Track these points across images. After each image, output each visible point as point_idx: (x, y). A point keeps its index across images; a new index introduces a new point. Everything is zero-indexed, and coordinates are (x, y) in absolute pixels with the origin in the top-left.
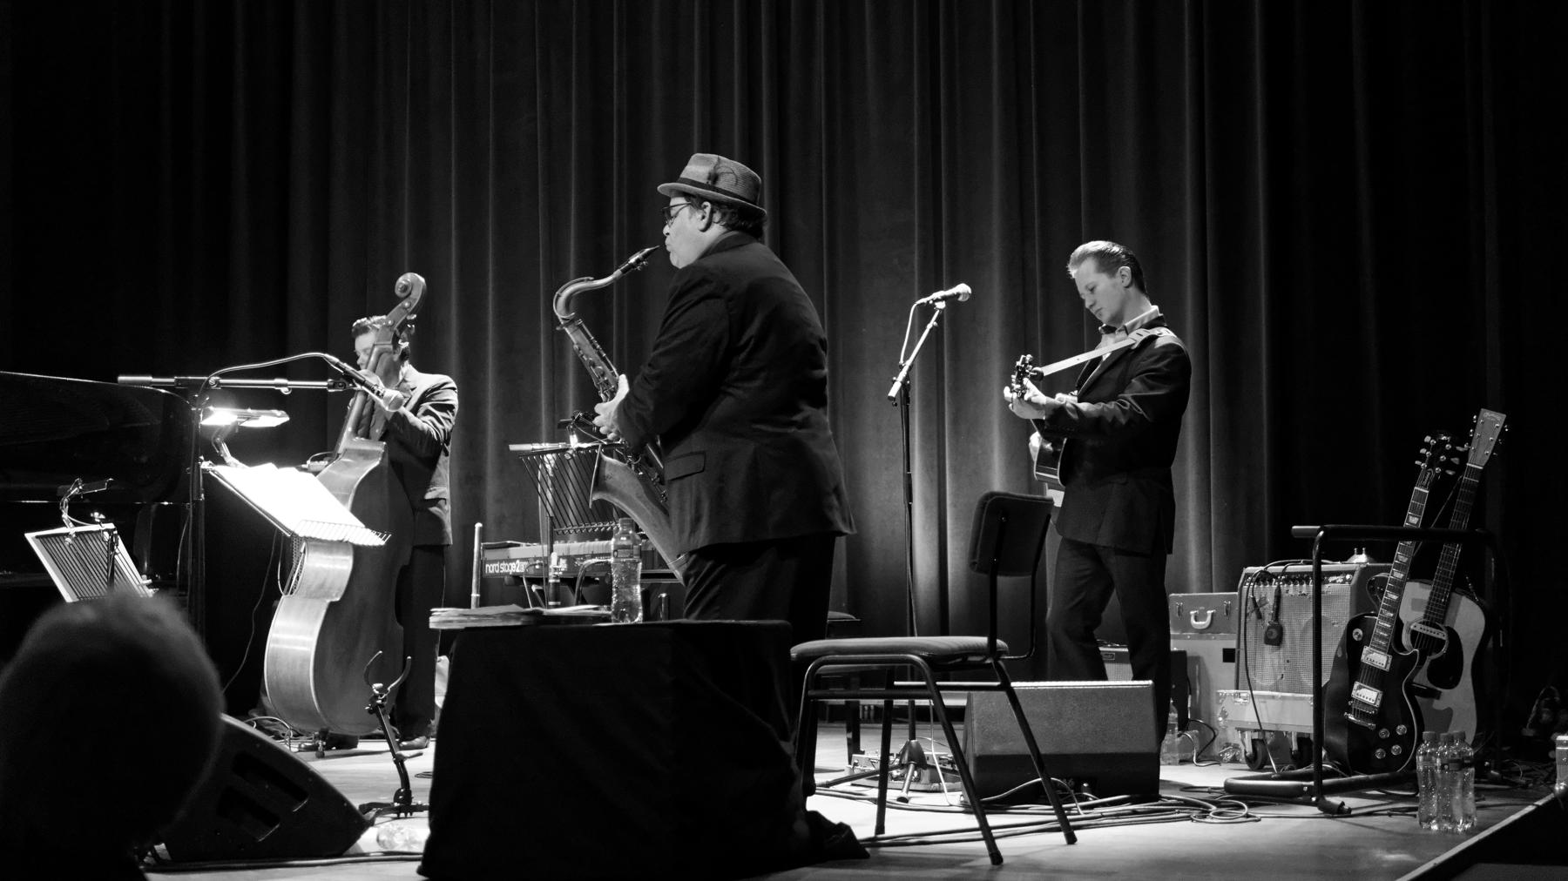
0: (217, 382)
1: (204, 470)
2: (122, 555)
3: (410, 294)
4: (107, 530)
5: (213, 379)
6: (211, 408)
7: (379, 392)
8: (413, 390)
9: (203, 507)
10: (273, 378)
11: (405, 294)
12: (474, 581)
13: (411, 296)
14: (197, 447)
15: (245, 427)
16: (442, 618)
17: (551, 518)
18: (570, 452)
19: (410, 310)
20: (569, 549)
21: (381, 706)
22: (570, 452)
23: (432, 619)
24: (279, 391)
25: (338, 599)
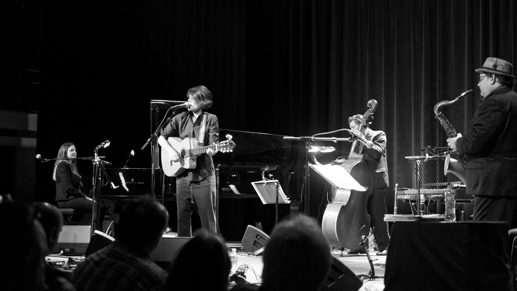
0: (314, 139)
1: (309, 166)
2: (281, 190)
3: (372, 106)
4: (276, 182)
5: (312, 138)
6: (312, 146)
7: (365, 142)
8: (371, 137)
9: (309, 178)
10: (331, 137)
11: (370, 106)
12: (395, 203)
13: (372, 107)
14: (307, 159)
15: (321, 153)
16: (387, 218)
17: (419, 181)
18: (426, 159)
19: (372, 111)
20: (425, 191)
21: (365, 243)
22: (426, 159)
23: (385, 218)
24: (333, 141)
25: (345, 205)
